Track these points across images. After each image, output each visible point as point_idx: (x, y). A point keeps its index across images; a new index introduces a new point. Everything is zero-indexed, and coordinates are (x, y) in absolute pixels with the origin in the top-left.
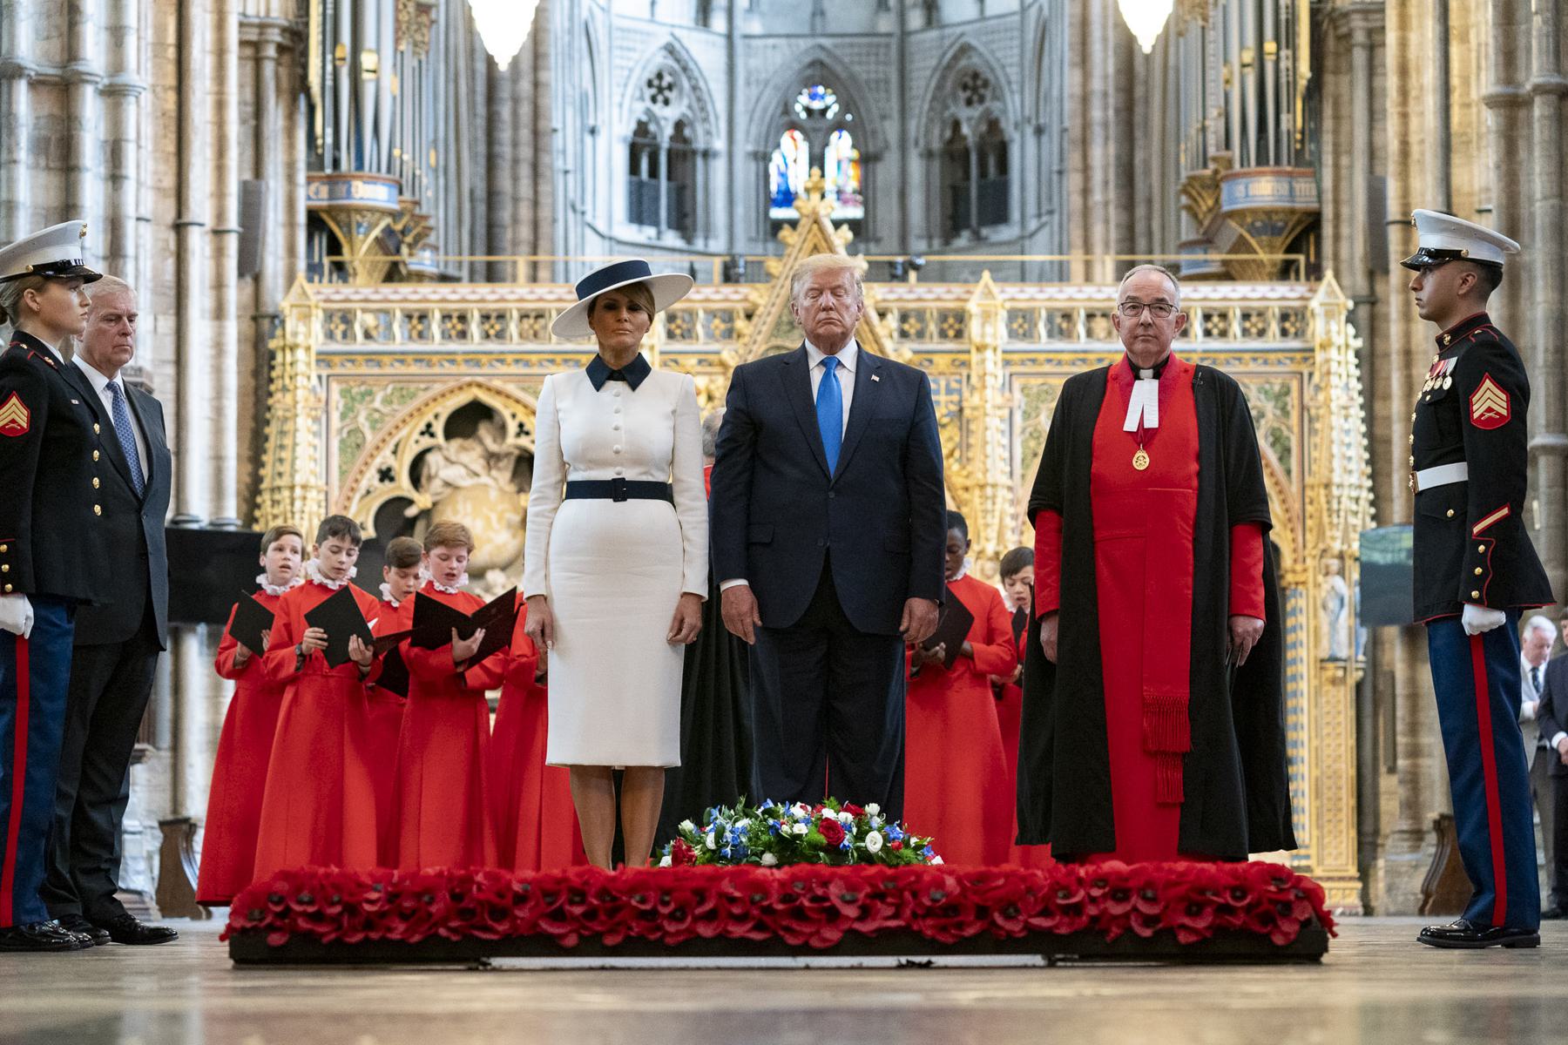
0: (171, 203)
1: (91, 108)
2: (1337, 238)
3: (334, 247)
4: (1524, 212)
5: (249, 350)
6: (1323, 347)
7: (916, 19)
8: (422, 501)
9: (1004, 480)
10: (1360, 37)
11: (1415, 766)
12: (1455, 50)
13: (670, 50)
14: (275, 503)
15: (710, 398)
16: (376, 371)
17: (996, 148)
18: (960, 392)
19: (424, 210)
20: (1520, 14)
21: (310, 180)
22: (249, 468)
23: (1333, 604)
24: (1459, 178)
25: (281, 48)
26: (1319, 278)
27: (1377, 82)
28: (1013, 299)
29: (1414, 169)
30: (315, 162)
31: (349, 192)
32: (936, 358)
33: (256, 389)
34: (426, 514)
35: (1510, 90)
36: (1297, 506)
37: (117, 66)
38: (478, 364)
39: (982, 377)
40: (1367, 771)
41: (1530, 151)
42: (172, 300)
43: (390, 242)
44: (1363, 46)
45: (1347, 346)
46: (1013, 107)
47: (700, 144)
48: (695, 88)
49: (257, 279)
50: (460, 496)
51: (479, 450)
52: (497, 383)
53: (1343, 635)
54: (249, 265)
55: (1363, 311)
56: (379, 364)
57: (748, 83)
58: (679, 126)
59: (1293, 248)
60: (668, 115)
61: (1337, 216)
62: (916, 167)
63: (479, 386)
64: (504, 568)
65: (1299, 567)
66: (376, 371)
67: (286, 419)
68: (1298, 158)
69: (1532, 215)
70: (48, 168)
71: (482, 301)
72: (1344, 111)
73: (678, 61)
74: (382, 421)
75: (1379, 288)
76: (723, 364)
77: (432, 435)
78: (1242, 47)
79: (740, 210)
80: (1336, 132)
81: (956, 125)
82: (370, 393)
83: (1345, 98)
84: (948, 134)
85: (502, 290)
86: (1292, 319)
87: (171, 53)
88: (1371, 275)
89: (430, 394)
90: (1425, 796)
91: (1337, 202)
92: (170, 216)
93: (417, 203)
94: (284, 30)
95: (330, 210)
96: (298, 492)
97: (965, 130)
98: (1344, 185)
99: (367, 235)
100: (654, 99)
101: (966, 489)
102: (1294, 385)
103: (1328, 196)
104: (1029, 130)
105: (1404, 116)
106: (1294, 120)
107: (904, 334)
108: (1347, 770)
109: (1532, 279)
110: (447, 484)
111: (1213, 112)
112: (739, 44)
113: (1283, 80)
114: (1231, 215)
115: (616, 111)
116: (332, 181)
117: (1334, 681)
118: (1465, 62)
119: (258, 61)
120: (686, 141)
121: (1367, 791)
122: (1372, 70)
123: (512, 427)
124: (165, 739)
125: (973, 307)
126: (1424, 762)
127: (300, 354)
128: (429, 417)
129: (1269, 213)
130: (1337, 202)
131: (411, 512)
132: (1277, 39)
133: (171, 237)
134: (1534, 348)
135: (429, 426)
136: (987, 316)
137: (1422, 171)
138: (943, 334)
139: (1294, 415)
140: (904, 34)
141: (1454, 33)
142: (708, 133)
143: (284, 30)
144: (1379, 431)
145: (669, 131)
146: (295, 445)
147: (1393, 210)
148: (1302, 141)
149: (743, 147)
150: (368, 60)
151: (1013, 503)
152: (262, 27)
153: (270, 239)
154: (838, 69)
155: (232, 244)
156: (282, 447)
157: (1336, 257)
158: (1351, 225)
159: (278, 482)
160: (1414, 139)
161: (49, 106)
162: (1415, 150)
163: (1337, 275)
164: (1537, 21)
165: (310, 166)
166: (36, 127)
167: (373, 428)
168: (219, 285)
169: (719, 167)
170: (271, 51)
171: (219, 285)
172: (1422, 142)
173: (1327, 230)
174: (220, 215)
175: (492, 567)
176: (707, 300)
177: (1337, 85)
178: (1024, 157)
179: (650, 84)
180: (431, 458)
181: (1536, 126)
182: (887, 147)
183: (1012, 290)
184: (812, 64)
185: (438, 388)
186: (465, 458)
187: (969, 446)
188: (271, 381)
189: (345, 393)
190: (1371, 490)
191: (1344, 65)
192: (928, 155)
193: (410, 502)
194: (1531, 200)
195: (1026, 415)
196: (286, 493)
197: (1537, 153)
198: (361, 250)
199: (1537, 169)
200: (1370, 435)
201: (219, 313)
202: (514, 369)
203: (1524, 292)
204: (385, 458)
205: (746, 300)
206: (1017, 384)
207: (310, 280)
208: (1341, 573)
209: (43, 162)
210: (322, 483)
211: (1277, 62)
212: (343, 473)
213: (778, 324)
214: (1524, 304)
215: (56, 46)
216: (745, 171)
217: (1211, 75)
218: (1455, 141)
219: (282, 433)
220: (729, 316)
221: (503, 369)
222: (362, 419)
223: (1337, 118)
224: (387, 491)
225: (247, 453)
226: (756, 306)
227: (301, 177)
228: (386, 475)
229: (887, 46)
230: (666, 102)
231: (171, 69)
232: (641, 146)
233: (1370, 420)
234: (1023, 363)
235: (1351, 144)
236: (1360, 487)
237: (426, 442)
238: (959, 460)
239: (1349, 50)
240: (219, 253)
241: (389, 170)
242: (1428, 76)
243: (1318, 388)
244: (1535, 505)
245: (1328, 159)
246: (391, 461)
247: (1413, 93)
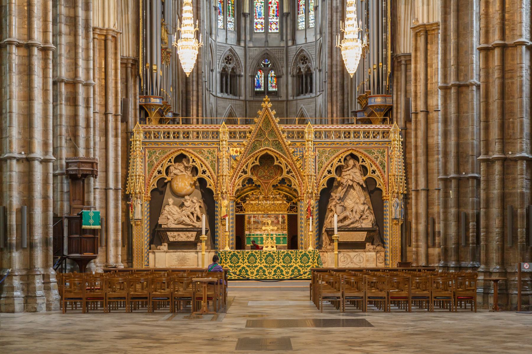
0: (104, 108)
1: (81, 90)
2: (397, 113)
3: (147, 115)
4: (449, 117)
5: (125, 140)
6: (394, 141)
7: (290, 43)
8: (169, 179)
9: (314, 174)
10: (403, 62)
11: (417, 250)
12: (429, 69)
13: (230, 50)
14: (132, 179)
15: (240, 153)
16: (157, 146)
17: (309, 74)
18: (303, 152)
19: (169, 104)
20: (448, 65)
21: (140, 98)
22: (125, 170)
23: (396, 205)
24: (431, 102)
25: (132, 65)
26: (392, 123)
27: (408, 73)
28: (316, 128)
29: (418, 99)
30: (141, 93)
31: (150, 100)
32: (297, 143)
33: (127, 151)
34: (170, 182)
35: (445, 85)
36: (387, 180)
37: (88, 78)
38: (182, 144)
39: (308, 148)
40: (404, 246)
41: (451, 101)
42: (104, 133)
43: (161, 113)
44: (404, 64)
45: (400, 140)
46: (314, 65)
47: (238, 73)
48: (237, 60)
49: (127, 123)
50: (178, 177)
51: (183, 166)
52: (187, 149)
53: (398, 213)
54: (125, 120)
55: (403, 131)
56: (158, 145)
57: (249, 59)
58: (233, 69)
59: (386, 115)
60: (231, 66)
61: (397, 107)
62: (290, 79)
63: (183, 150)
64: (189, 195)
65: (387, 195)
66: (157, 146)
67: (134, 159)
68: (387, 92)
69: (451, 117)
70: (70, 105)
71: (183, 129)
72: (399, 81)
73: (232, 53)
74: (158, 159)
75: (408, 125)
76: (244, 145)
77: (171, 162)
78: (374, 64)
79: (248, 89)
80: (397, 86)
81: (300, 69)
82: (155, 152)
83: (399, 78)
84: (298, 71)
85: (189, 126)
86: (385, 134)
87: (103, 70)
88: (405, 123)
89: (170, 152)
90: (420, 258)
91: (397, 104)
92: (104, 111)
93: (168, 102)
94: (133, 60)
95: (145, 105)
96: (138, 177)
97: (302, 70)
98: (399, 99)
99: (154, 111)
100: (227, 63)
101: (304, 176)
102: (386, 150)
103: (395, 102)
104: (317, 70)
105: (416, 86)
106: (386, 83)
107: (288, 137)
108: (399, 246)
109: (450, 134)
110: (175, 174)
111: (366, 80)
112: (247, 49)
113: (384, 73)
114: (370, 106)
115: (217, 66)
116: (145, 98)
117: (396, 224)
118: (431, 72)
119: (127, 68)
120: (234, 72)
121: (404, 251)
122: (406, 71)
123: (191, 160)
124: (104, 243)
125: (306, 130)
126: (420, 249)
127: (138, 142)
128: (170, 158)
129: (380, 106)
130: (397, 104)
131: (166, 181)
132: (382, 62)
133: (104, 117)
134: (451, 151)
135: (170, 160)
136: (309, 133)
137: (420, 100)
138: (298, 137)
139: (386, 157)
140: (287, 47)
141: (429, 65)
143: (133, 60)
144: (408, 161)
145: (230, 70)
146: (136, 169)
147: (413, 110)
148: (388, 88)
149: (249, 74)
150: (154, 67)
151: (316, 180)
152: (127, 59)
153: (130, 113)
154: (271, 55)
155: (119, 118)
156: (133, 165)
157: (397, 117)
158: (401, 109)
159: (132, 174)
160: (418, 92)
161: (70, 89)
162: (419, 95)
163: (397, 123)
164: (453, 68)
165: (140, 94)
166: (67, 95)
167: (156, 161)
168: (116, 129)
169: (243, 79)
170: (130, 65)
171: (116, 129)
172: (420, 92)
173: (395, 111)
174: (116, 111)
175: (186, 195)
176: (240, 129)
177: (397, 74)
178: (317, 77)
179: (226, 59)
180: (171, 168)
181: (452, 94)
182: (283, 74)
183: (316, 126)
184: (265, 54)
185: (172, 150)
186: (179, 168)
187: (305, 165)
188: (131, 149)
189: (149, 152)
190: (405, 176)
191: (399, 68)
192: (293, 76)
193: (166, 179)
194: (450, 113)
195: (319, 157)
196: (134, 177)
197: (452, 101)
198: (153, 115)
199: (452, 106)
200: (405, 163)
201: (116, 136)
202: (191, 146)
203: (449, 137)
204: (159, 168)
205: (249, 128)
206: (317, 150)
207: (140, 123)
208: (398, 197)
209: (69, 104)
210: (143, 175)
211: (382, 68)
212: (149, 172)
213: (257, 135)
214: (448, 140)
215: (72, 74)
216: (249, 80)
217: (365, 70)
218: (429, 93)
219: (134, 162)
220: (245, 133)
221: (189, 146)
222: (153, 158)
223: (397, 82)
224: (159, 176)
225: (124, 166)
226: (252, 130)
227: (138, 97)
228: (159, 172)
229: (283, 49)
230: (230, 63)
231: (103, 74)
232: (224, 74)
233: (405, 158)
234: (318, 144)
235: (401, 89)
236: (402, 176)
237: (169, 164)
238: (302, 169)
239: (401, 65)
240: (116, 120)
241: (160, 95)
242: (422, 76)
243: (392, 151)
244: (451, 192)
245: (395, 93)
246: (161, 169)
247: (418, 80)
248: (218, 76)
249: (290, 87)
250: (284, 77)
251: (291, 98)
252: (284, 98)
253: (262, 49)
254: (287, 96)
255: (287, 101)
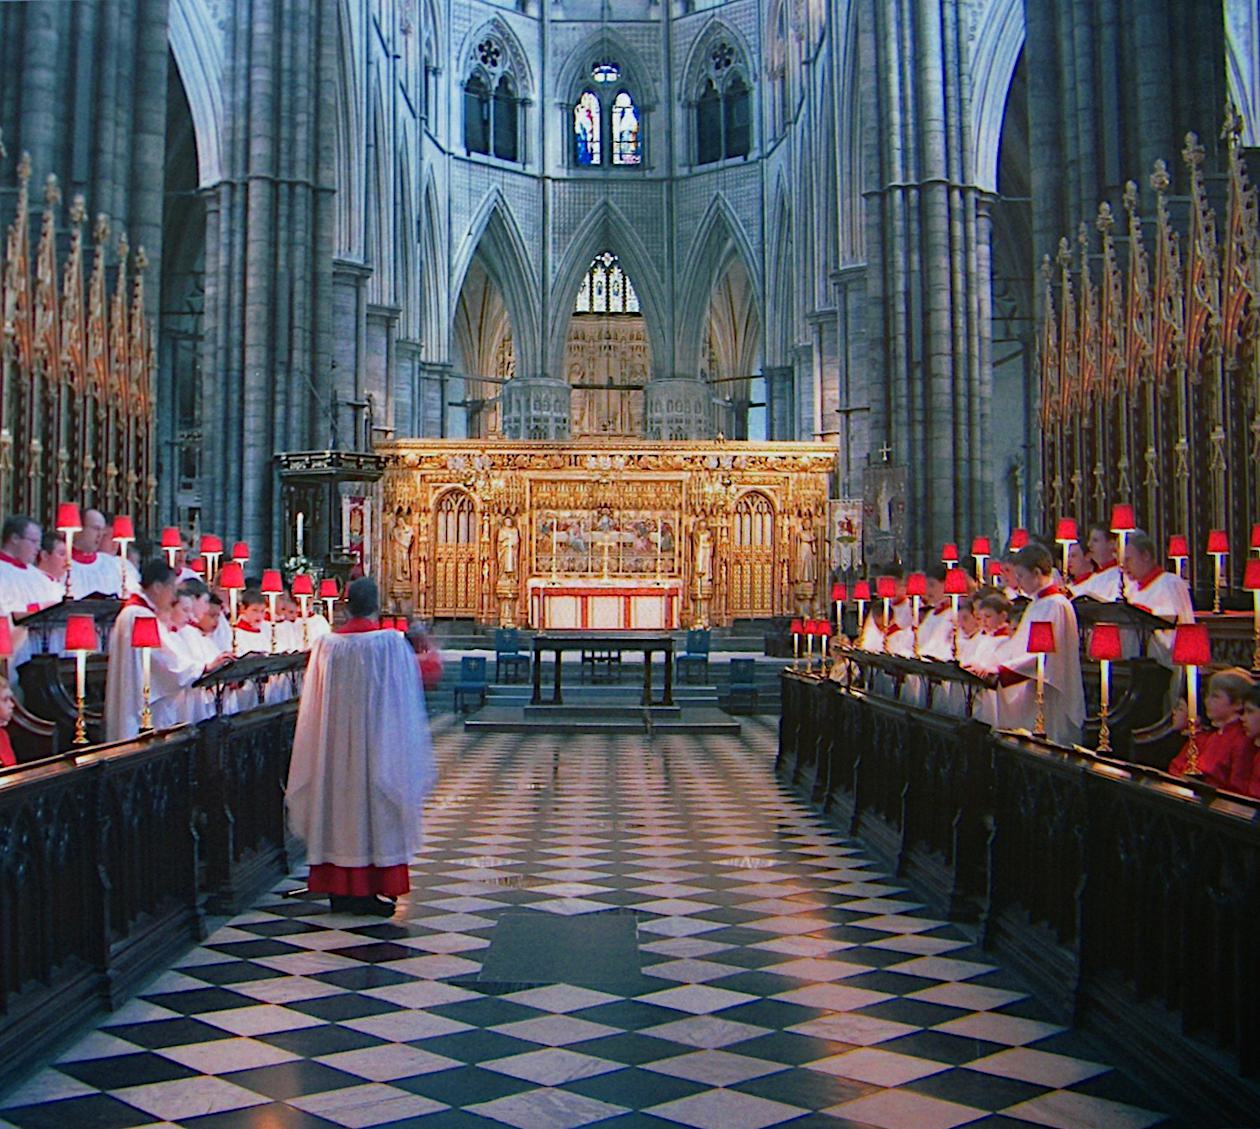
17: (739, 92)
47: (520, 95)
48: (516, 54)
58: (503, 80)
60: (498, 71)
62: (679, 114)
73: (502, 33)
81: (710, 82)
84: (703, 90)
97: (715, 86)
100: (484, 59)
104: (765, 77)
115: (454, 63)
120: (508, 92)
140: (669, 21)
142: (526, 87)
145: (495, 84)
154: (622, 45)
178: (764, 100)
179: (481, 48)
182: (657, 102)
184: (602, 41)
192: (688, 105)
229: (657, 29)
230: (494, 63)
248: (457, 95)
249: (679, 138)
250: (660, 112)
251: (681, 172)
252: (660, 172)
253: (594, 25)
254: (670, 167)
255: (671, 179)
